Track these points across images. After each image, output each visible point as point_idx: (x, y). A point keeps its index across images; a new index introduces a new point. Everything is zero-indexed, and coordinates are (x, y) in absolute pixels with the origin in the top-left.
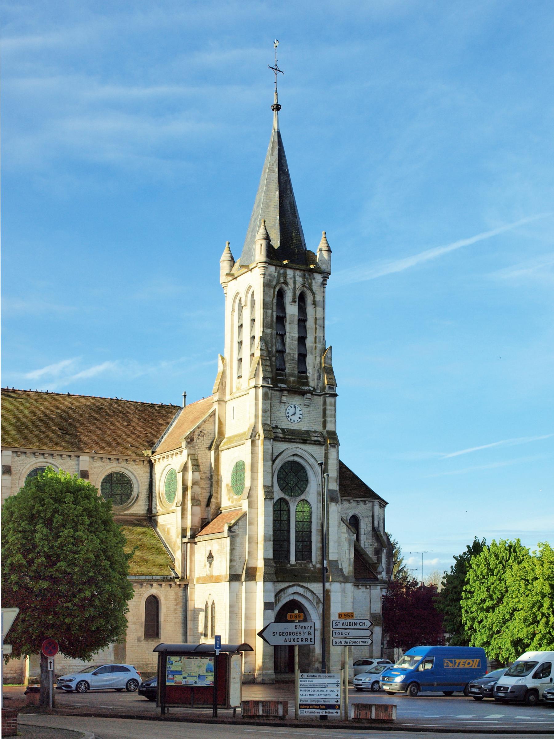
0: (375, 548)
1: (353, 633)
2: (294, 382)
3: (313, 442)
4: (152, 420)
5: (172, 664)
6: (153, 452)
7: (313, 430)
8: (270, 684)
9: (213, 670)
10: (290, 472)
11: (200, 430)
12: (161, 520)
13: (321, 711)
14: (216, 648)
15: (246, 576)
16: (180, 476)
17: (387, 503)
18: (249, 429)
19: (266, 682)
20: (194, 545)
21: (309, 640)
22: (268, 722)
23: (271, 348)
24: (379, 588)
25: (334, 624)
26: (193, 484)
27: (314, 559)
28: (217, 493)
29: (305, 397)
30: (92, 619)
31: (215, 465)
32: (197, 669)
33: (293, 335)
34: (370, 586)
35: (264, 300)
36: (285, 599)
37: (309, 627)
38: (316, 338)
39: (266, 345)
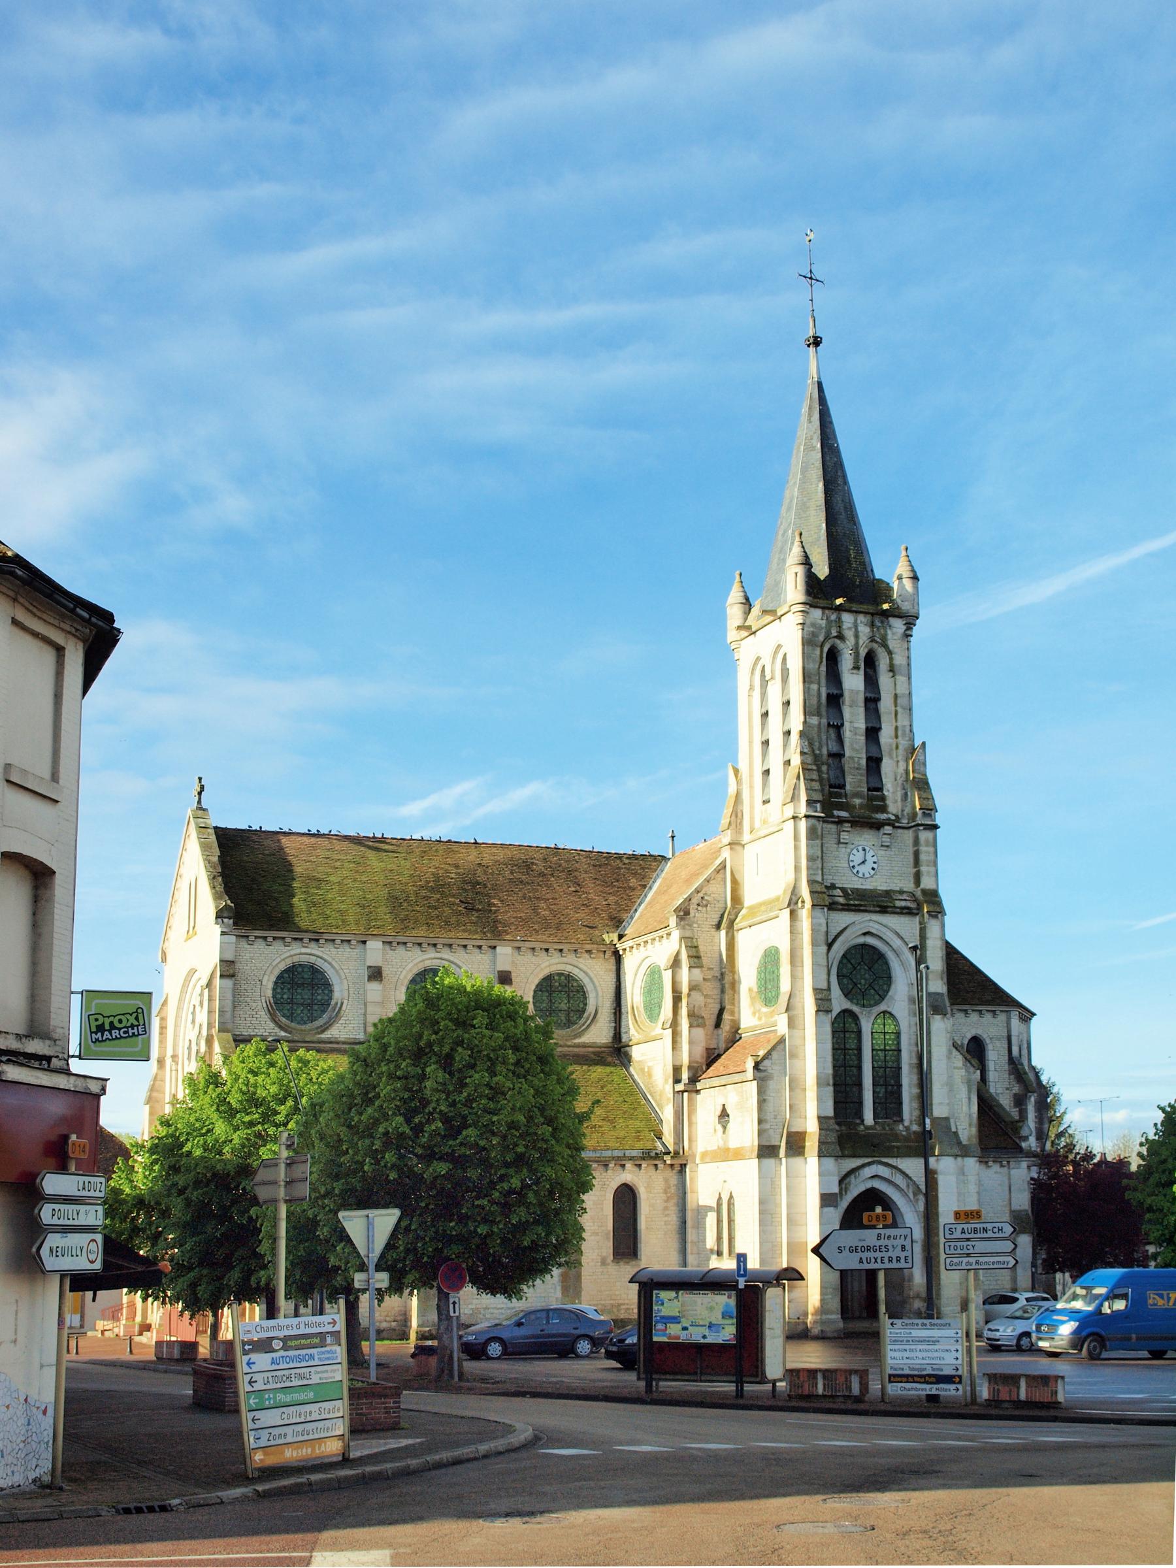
0: (1015, 1095)
1: (981, 1247)
2: (861, 806)
3: (898, 910)
4: (618, 881)
5: (662, 1304)
6: (621, 937)
7: (898, 889)
8: (835, 1338)
9: (735, 1314)
10: (859, 964)
11: (701, 895)
12: (636, 1053)
13: (928, 1387)
14: (739, 1275)
15: (787, 1148)
16: (667, 976)
17: (1033, 1014)
18: (785, 891)
19: (829, 1335)
20: (694, 1095)
21: (903, 1260)
22: (835, 1406)
23: (820, 749)
24: (1024, 1165)
25: (947, 1232)
26: (690, 990)
28: (733, 1004)
29: (882, 831)
30: (523, 1227)
31: (728, 956)
32: (705, 1313)
33: (856, 725)
34: (1008, 1162)
35: (804, 668)
36: (857, 1187)
37: (903, 1237)
38: (896, 728)
39: (811, 744)
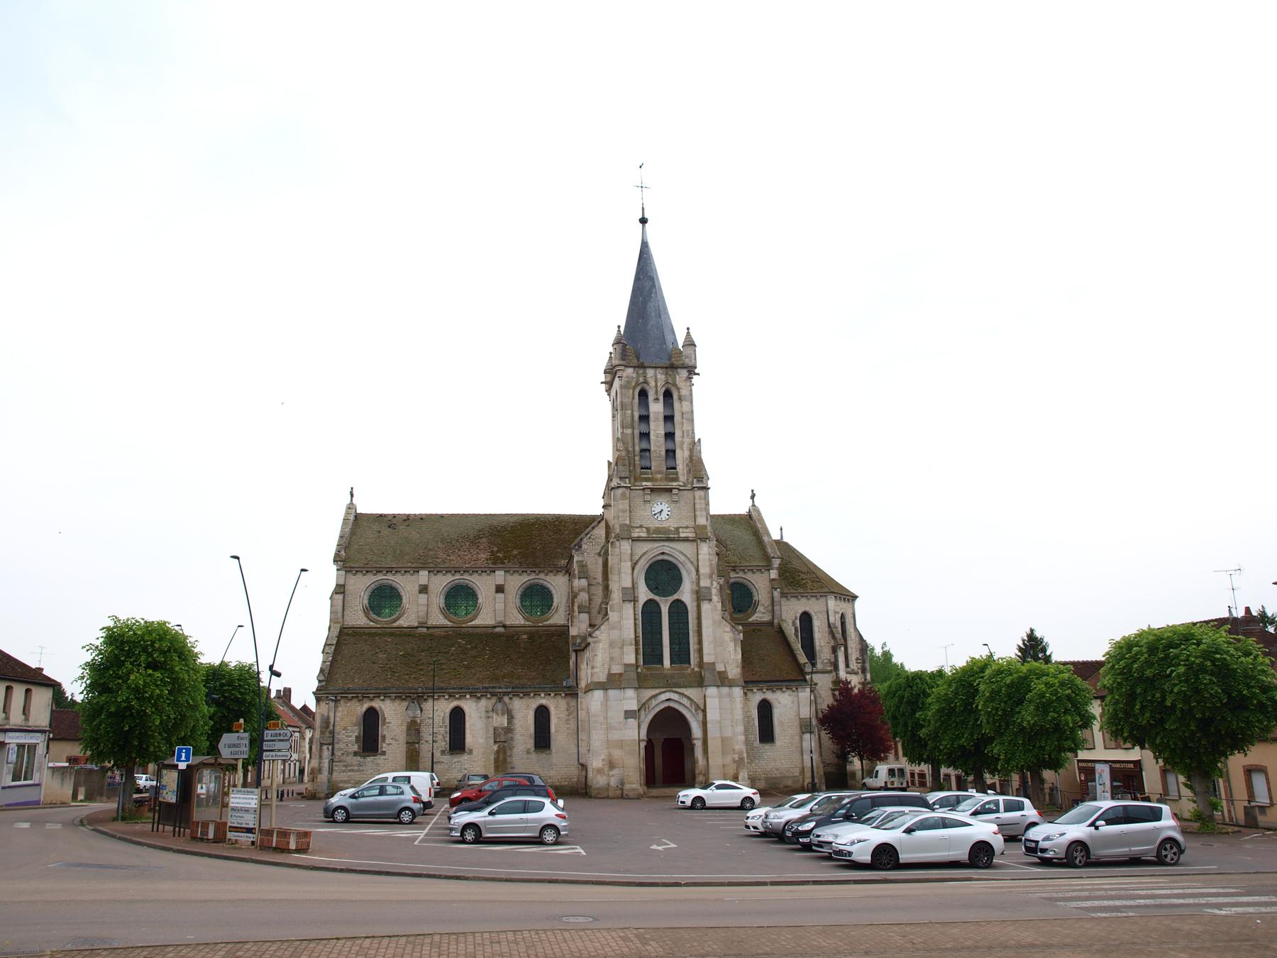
0: (833, 647)
27: (692, 662)
36: (657, 706)
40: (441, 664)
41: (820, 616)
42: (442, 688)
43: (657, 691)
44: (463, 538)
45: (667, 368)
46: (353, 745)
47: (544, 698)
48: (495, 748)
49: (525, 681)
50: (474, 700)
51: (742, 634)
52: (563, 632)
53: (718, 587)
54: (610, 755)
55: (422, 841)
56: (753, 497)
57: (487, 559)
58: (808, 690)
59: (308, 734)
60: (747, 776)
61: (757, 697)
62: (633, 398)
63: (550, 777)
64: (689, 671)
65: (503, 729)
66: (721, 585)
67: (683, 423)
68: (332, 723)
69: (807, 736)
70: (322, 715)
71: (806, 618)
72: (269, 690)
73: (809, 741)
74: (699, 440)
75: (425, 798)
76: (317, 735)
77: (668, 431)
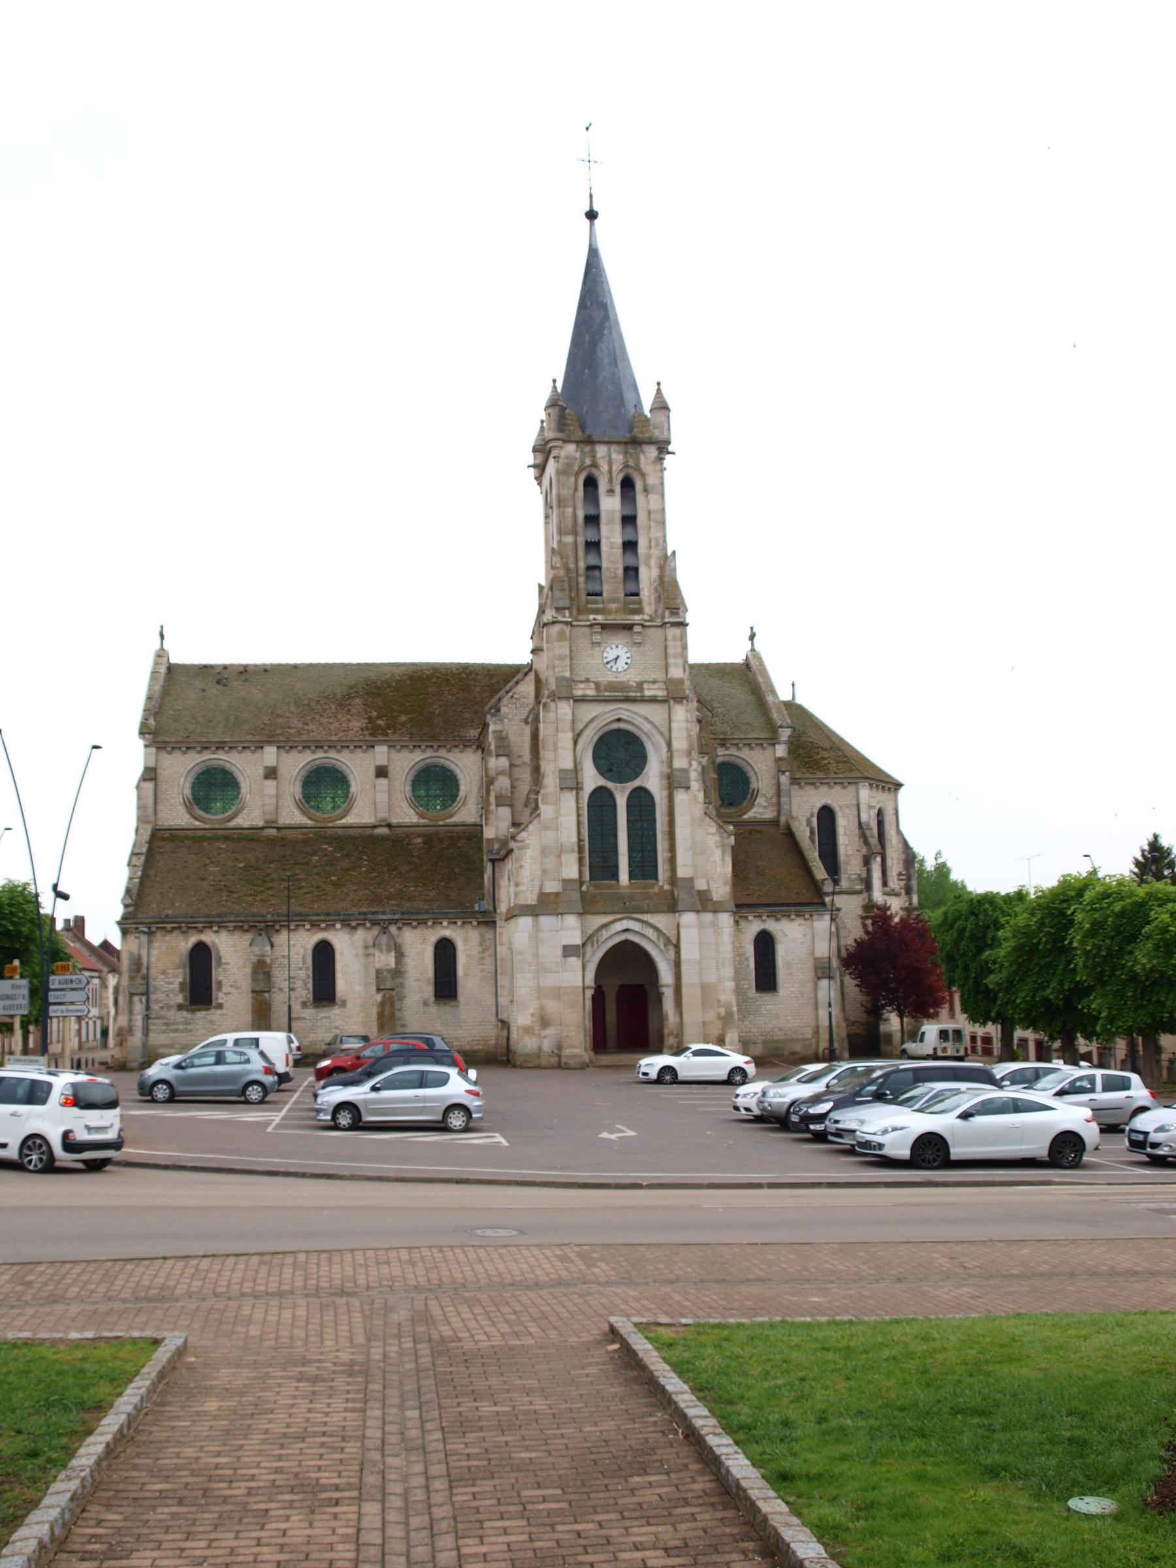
40: (298, 880)
41: (847, 811)
42: (300, 915)
43: (609, 918)
44: (327, 698)
45: (626, 443)
46: (176, 995)
47: (447, 927)
48: (379, 998)
49: (421, 904)
50: (348, 930)
51: (733, 837)
52: (473, 834)
53: (700, 769)
54: (542, 1008)
55: (278, 1127)
56: (752, 637)
57: (362, 729)
58: (827, 917)
59: (112, 981)
60: (737, 1039)
61: (753, 927)
62: (576, 489)
63: (457, 1039)
64: (656, 889)
65: (389, 971)
66: (703, 768)
67: (650, 527)
68: (145, 965)
69: (824, 983)
70: (131, 954)
71: (827, 816)
72: (53, 920)
73: (827, 990)
74: (674, 553)
75: (281, 1068)
76: (125, 982)
77: (627, 539)
